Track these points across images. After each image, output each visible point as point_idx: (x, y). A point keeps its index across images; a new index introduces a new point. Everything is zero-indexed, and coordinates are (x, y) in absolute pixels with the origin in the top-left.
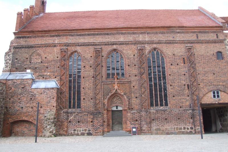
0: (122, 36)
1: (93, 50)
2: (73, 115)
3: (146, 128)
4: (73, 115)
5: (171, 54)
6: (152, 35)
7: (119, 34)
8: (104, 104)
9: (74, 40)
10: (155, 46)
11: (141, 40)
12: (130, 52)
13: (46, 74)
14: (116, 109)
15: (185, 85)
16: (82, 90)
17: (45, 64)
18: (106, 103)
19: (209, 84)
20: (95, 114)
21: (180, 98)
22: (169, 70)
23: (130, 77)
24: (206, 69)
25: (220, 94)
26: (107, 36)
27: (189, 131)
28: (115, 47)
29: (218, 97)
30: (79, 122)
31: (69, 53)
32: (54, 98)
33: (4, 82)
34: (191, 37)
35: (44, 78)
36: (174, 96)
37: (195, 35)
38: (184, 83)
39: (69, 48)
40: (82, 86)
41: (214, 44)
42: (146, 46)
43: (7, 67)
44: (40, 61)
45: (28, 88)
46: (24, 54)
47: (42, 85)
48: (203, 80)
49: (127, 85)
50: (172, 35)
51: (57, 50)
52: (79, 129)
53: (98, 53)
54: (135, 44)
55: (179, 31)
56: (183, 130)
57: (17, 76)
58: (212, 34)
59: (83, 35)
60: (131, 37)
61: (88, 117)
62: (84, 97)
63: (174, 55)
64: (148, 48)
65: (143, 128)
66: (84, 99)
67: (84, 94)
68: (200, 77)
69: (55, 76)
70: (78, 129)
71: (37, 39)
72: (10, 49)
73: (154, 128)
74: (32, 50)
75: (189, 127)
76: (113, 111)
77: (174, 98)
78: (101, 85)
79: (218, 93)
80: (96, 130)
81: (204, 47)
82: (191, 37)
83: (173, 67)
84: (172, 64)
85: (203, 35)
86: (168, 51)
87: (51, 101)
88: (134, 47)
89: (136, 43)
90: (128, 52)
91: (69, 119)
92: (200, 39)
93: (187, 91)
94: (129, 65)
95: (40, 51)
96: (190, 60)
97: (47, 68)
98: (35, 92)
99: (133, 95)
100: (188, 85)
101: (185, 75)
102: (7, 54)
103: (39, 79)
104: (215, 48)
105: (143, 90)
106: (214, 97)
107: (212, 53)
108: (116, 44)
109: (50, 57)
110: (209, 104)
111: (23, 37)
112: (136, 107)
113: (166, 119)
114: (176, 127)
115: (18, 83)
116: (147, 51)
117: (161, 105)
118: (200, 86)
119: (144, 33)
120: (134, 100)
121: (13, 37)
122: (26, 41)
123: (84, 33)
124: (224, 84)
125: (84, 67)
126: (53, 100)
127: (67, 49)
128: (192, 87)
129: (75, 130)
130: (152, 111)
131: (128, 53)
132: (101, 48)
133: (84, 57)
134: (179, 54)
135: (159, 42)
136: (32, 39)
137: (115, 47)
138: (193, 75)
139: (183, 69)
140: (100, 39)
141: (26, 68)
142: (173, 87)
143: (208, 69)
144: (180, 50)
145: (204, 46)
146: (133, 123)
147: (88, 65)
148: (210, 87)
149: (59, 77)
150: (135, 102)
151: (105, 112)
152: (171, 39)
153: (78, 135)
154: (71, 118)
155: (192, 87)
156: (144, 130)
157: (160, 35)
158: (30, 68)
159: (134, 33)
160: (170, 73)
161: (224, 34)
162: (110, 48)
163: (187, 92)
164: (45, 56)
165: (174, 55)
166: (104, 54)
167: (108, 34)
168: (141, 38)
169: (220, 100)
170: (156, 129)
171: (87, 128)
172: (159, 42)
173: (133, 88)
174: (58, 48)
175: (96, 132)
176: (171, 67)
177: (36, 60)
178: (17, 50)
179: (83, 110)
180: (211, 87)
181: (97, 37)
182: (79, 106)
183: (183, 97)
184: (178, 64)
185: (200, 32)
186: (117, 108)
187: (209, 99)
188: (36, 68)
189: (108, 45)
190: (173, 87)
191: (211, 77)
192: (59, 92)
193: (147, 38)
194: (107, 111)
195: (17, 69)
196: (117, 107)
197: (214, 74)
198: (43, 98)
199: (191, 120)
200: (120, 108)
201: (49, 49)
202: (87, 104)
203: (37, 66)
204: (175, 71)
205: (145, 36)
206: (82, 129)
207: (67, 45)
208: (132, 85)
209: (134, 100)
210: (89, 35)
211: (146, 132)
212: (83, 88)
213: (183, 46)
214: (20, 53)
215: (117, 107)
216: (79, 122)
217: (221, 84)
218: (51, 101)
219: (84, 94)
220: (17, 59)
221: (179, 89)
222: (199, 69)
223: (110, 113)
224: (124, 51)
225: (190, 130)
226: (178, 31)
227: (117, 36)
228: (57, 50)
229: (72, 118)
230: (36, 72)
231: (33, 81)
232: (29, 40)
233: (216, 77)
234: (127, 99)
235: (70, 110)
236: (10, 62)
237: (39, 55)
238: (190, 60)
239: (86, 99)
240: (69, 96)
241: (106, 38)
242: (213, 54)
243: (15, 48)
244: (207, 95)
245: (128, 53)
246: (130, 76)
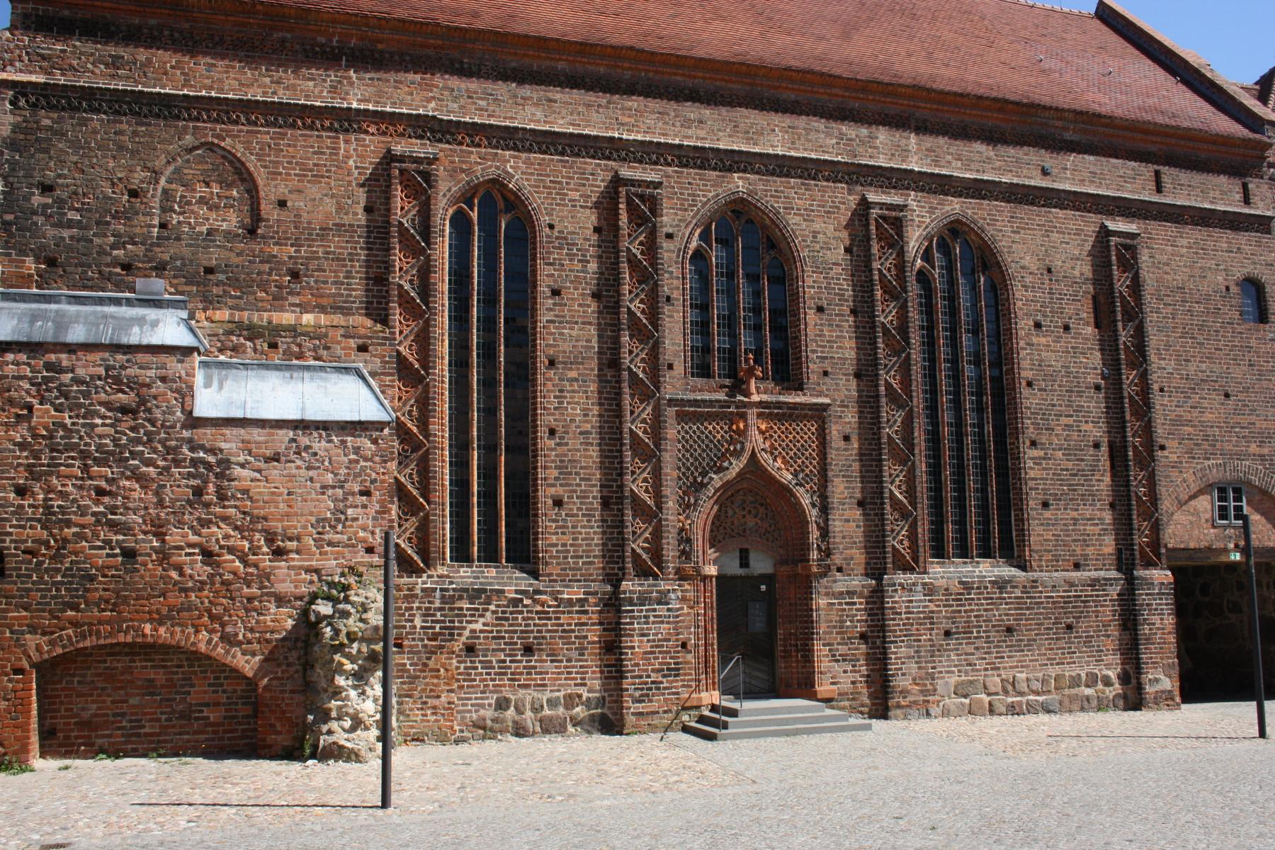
2: (492, 607)
3: (914, 679)
4: (492, 607)
5: (1033, 268)
9: (483, 103)
12: (816, 226)
13: (287, 318)
14: (741, 566)
15: (1097, 446)
17: (275, 250)
19: (1206, 446)
21: (1075, 514)
23: (827, 380)
24: (1192, 367)
26: (692, 111)
30: (528, 650)
32: (366, 493)
36: (1045, 505)
37: (1147, 170)
40: (545, 420)
42: (913, 200)
45: (167, 408)
48: (1178, 422)
52: (528, 696)
56: (1089, 691)
60: (828, 135)
61: (584, 619)
62: (558, 490)
63: (1049, 271)
66: (558, 503)
67: (555, 473)
69: (360, 341)
70: (522, 692)
73: (953, 680)
77: (1047, 514)
80: (640, 702)
81: (1185, 242)
83: (1043, 340)
84: (1038, 325)
85: (1184, 176)
87: (350, 511)
90: (817, 226)
91: (467, 633)
94: (820, 309)
97: (295, 275)
98: (223, 445)
103: (235, 349)
104: (1236, 256)
113: (1009, 630)
114: (1053, 671)
115: (81, 372)
118: (1166, 453)
120: (848, 521)
122: (115, 62)
124: (1266, 451)
125: (556, 293)
126: (364, 507)
129: (502, 705)
131: (815, 234)
133: (551, 227)
134: (1073, 268)
137: (739, 183)
140: (650, 121)
141: (127, 267)
142: (1042, 453)
143: (1204, 366)
146: (843, 649)
147: (577, 281)
148: (1207, 463)
153: (520, 731)
154: (478, 626)
156: (905, 693)
158: (160, 269)
160: (1027, 374)
164: (282, 190)
165: (1049, 271)
168: (885, 147)
170: (962, 683)
171: (581, 690)
172: (978, 190)
173: (842, 444)
175: (642, 714)
176: (1035, 340)
177: (203, 211)
178: (47, 122)
179: (551, 574)
180: (1211, 462)
181: (634, 103)
183: (1088, 514)
184: (1066, 328)
186: (744, 563)
188: (209, 271)
190: (1042, 453)
191: (1213, 410)
193: (915, 153)
195: (51, 262)
197: (1227, 395)
198: (291, 493)
201: (303, 145)
203: (214, 256)
204: (1054, 361)
205: (904, 141)
206: (548, 695)
209: (848, 521)
211: (915, 702)
212: (552, 432)
213: (1088, 224)
214: (75, 144)
216: (528, 650)
217: (1253, 448)
218: (350, 511)
219: (555, 473)
220: (47, 189)
221: (1070, 465)
224: (793, 220)
225: (1117, 686)
229: (484, 624)
233: (1236, 412)
235: (465, 575)
239: (574, 505)
241: (687, 123)
242: (1227, 288)
245: (815, 234)
246: (826, 373)
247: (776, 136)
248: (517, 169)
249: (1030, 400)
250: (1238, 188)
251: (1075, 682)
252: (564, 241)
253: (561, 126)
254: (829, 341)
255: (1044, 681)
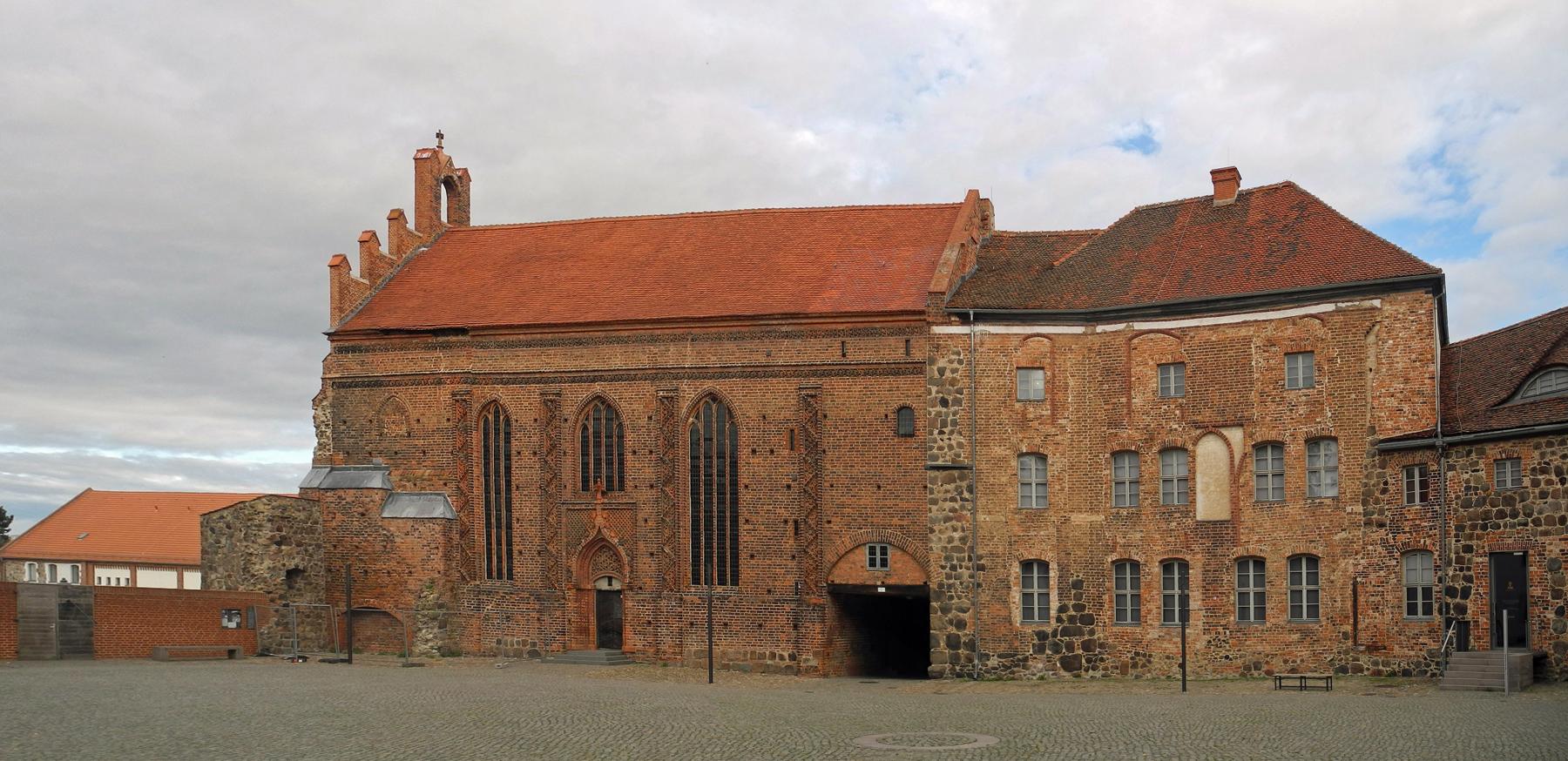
0: (618, 348)
1: (536, 397)
6: (706, 345)
7: (609, 341)
8: (569, 571)
10: (708, 385)
11: (671, 364)
12: (634, 403)
13: (419, 472)
15: (786, 522)
16: (515, 525)
18: (574, 569)
20: (545, 598)
22: (751, 468)
24: (855, 471)
25: (889, 557)
26: (577, 351)
27: (783, 664)
28: (597, 388)
29: (884, 563)
31: (477, 406)
33: (315, 496)
34: (822, 351)
35: (419, 486)
36: (752, 556)
38: (784, 513)
39: (478, 390)
40: (515, 515)
41: (892, 378)
42: (684, 385)
43: (321, 446)
44: (404, 430)
45: (373, 514)
46: (361, 404)
47: (407, 508)
49: (628, 514)
50: (767, 345)
51: (444, 394)
53: (551, 405)
54: (653, 379)
55: (790, 329)
57: (350, 476)
58: (892, 340)
59: (512, 345)
64: (689, 392)
65: (663, 647)
68: (830, 498)
71: (392, 355)
72: (323, 391)
74: (381, 395)
75: (786, 655)
76: (600, 591)
78: (559, 516)
79: (884, 551)
81: (858, 388)
82: (822, 351)
84: (754, 451)
86: (746, 400)
88: (648, 388)
89: (657, 374)
92: (850, 358)
93: (791, 542)
95: (403, 395)
96: (807, 436)
99: (641, 545)
100: (796, 522)
101: (789, 487)
102: (316, 402)
105: (667, 533)
106: (872, 563)
107: (882, 411)
108: (601, 379)
109: (430, 422)
110: (855, 586)
111: (354, 350)
112: (650, 583)
116: (684, 407)
117: (722, 582)
119: (683, 338)
121: (326, 347)
123: (514, 338)
127: (468, 393)
128: (807, 527)
130: (688, 598)
132: (559, 395)
135: (724, 373)
136: (379, 357)
137: (597, 388)
138: (811, 494)
139: (785, 466)
144: (780, 399)
145: (858, 385)
149: (453, 485)
150: (647, 566)
151: (571, 594)
152: (763, 360)
155: (807, 527)
156: (665, 653)
157: (730, 346)
159: (654, 340)
160: (746, 481)
161: (932, 337)
162: (583, 392)
163: (790, 544)
166: (569, 410)
167: (579, 343)
169: (887, 575)
172: (724, 373)
174: (449, 388)
182: (510, 577)
184: (772, 452)
185: (854, 333)
187: (856, 571)
189: (581, 380)
192: (455, 533)
194: (579, 590)
196: (610, 579)
199: (794, 634)
200: (616, 586)
201: (424, 393)
202: (527, 568)
207: (473, 379)
208: (641, 516)
210: (529, 344)
213: (791, 385)
215: (610, 579)
217: (895, 521)
222: (833, 467)
223: (592, 599)
224: (623, 404)
226: (784, 329)
227: (605, 349)
228: (444, 394)
230: (397, 467)
231: (389, 495)
232: (369, 357)
234: (626, 559)
236: (329, 432)
237: (400, 409)
238: (807, 436)
239: (526, 554)
240: (482, 547)
243: (339, 384)
244: (851, 557)
247: (617, 358)
248: (502, 394)
249: (745, 496)
250: (902, 345)
251: (762, 656)
252: (522, 428)
253: (521, 368)
254: (640, 469)
255: (745, 654)
